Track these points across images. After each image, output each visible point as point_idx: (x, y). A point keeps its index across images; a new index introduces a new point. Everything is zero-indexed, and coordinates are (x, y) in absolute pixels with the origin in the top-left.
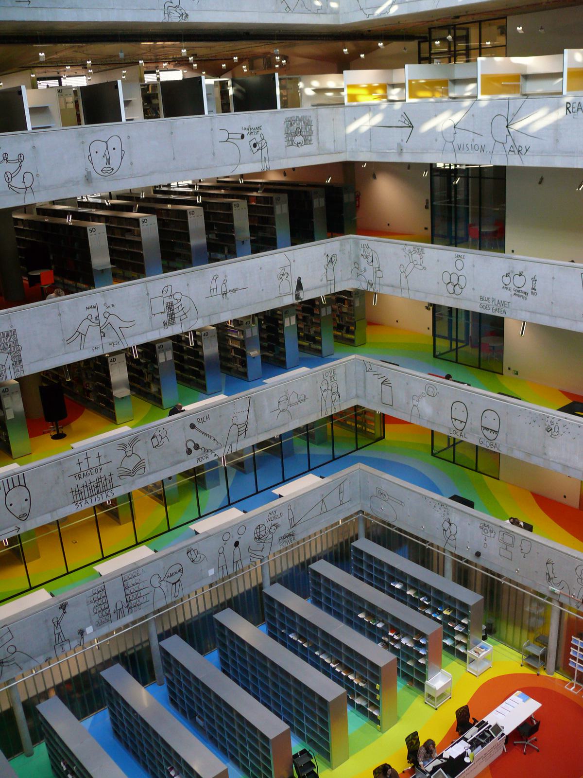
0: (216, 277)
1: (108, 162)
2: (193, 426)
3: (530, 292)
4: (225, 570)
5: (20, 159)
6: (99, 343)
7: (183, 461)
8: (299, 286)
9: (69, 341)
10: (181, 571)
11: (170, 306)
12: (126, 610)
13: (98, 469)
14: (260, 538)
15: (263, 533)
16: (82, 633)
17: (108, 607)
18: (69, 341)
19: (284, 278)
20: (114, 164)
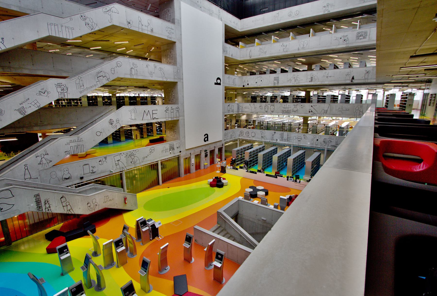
0: (326, 73)
1: (304, 46)
2: (312, 106)
4: (313, 145)
5: (286, 46)
6: (294, 83)
7: (308, 114)
8: (353, 78)
9: (288, 81)
10: (301, 139)
11: (312, 78)
12: (287, 140)
13: (288, 108)
14: (325, 142)
15: (326, 141)
16: (277, 140)
17: (283, 138)
18: (288, 81)
19: (348, 75)
20: (305, 46)
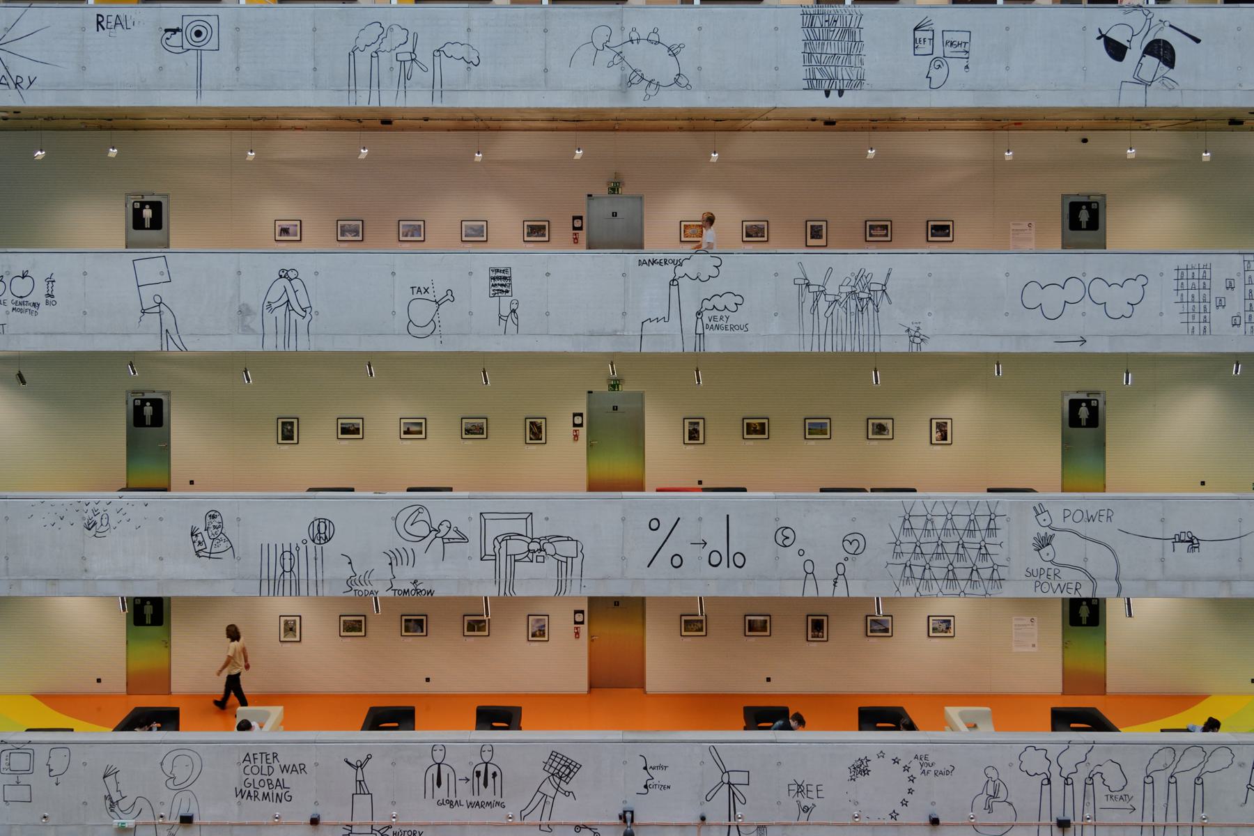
3: (42, 300)
